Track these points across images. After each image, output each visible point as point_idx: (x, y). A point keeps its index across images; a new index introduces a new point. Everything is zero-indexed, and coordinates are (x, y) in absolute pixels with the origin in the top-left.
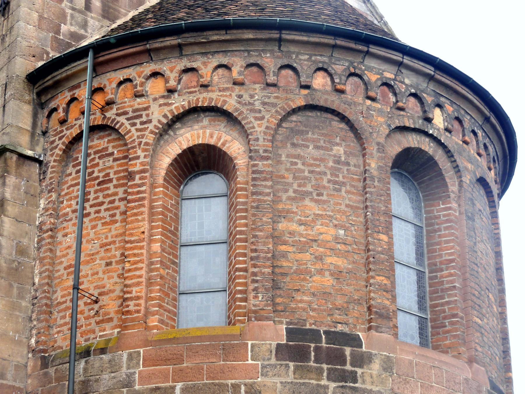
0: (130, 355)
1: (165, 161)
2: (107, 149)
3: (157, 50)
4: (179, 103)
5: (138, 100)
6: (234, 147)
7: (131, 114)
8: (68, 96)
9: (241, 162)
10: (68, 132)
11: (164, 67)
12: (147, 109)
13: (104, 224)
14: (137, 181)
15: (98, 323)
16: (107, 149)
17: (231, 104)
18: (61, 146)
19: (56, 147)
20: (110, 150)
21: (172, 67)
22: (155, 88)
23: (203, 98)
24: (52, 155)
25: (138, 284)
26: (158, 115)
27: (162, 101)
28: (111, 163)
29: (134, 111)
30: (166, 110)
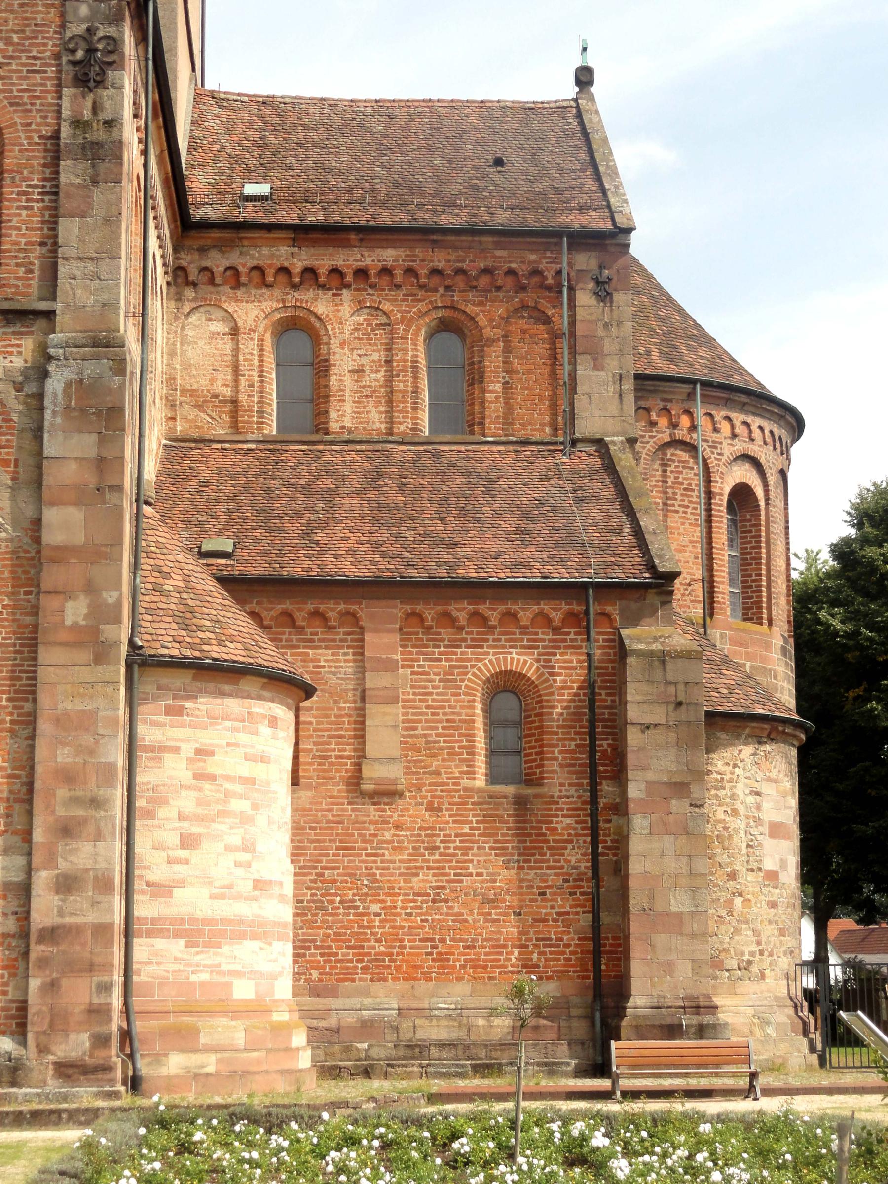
0: (721, 634)
1: (727, 490)
2: (688, 462)
3: (734, 401)
4: (740, 446)
5: (715, 435)
6: (759, 492)
7: (710, 444)
8: (661, 405)
9: (762, 503)
10: (660, 435)
11: (733, 415)
12: (721, 443)
13: (691, 524)
14: (717, 501)
15: (692, 602)
16: (688, 462)
17: (763, 461)
18: (651, 443)
19: (648, 442)
20: (691, 465)
21: (738, 418)
22: (725, 427)
23: (755, 450)
24: (644, 448)
25: (723, 583)
26: (729, 450)
27: (729, 441)
28: (692, 476)
29: (714, 442)
30: (732, 449)
